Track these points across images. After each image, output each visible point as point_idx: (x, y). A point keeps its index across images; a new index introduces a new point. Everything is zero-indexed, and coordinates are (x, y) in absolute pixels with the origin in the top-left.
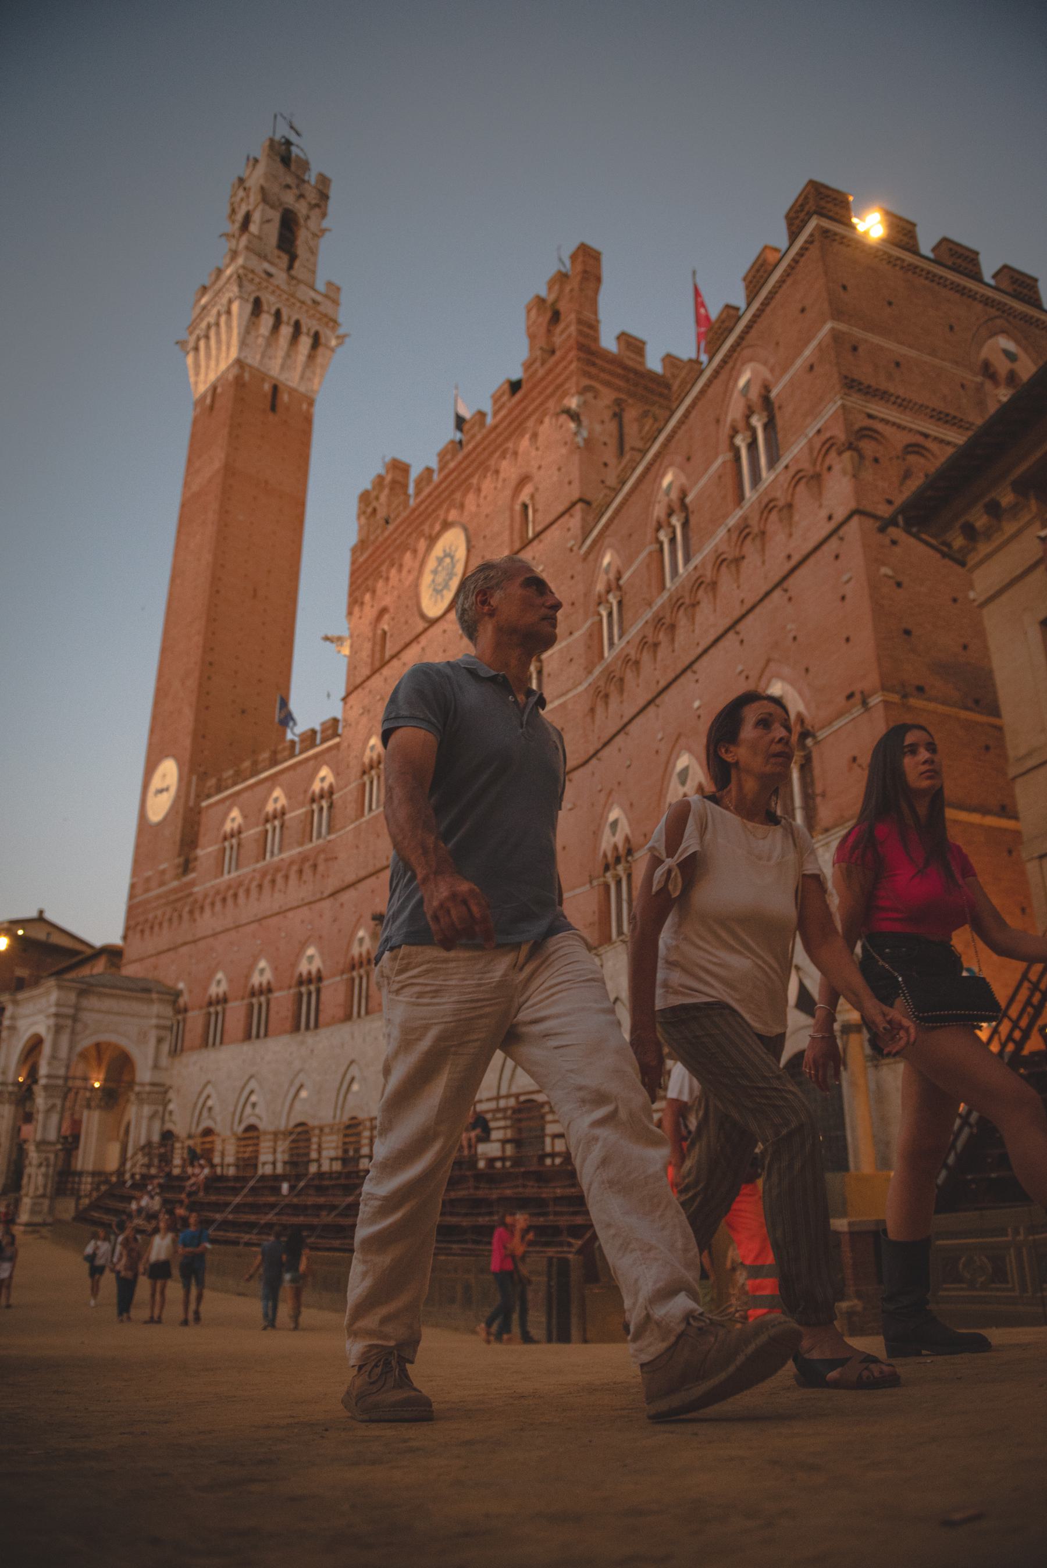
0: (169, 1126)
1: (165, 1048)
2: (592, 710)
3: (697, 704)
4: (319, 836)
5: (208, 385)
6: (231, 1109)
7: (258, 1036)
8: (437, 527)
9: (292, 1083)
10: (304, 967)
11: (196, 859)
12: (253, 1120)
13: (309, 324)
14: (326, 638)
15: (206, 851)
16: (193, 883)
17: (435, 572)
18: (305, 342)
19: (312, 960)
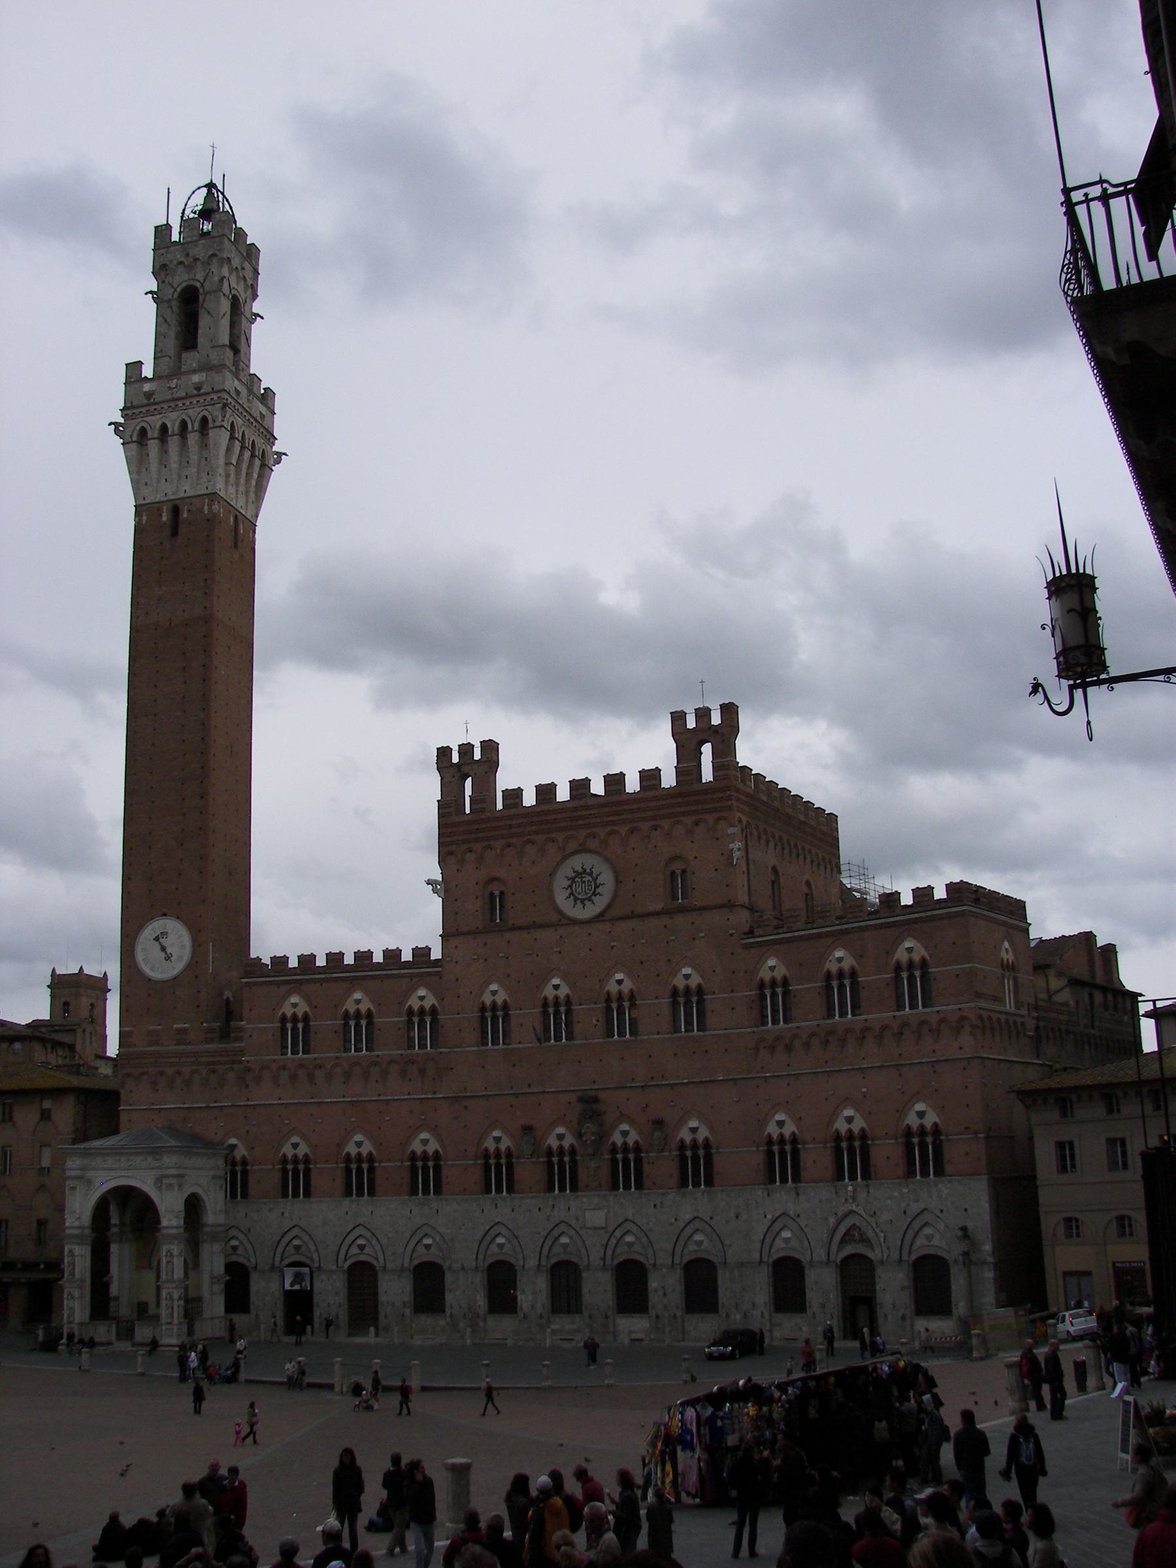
0: (234, 1258)
1: (221, 1195)
2: (757, 1050)
3: (864, 1090)
4: (422, 1046)
5: (160, 497)
6: (336, 1249)
7: (360, 1193)
8: (572, 846)
9: (414, 1234)
10: (417, 1147)
11: (241, 1029)
12: (362, 1258)
13: (260, 443)
14: (429, 882)
15: (257, 1028)
16: (242, 1052)
17: (573, 880)
18: (257, 462)
19: (425, 1142)
